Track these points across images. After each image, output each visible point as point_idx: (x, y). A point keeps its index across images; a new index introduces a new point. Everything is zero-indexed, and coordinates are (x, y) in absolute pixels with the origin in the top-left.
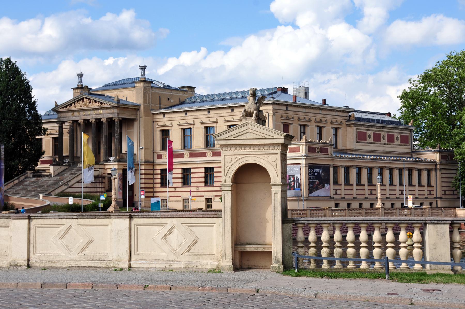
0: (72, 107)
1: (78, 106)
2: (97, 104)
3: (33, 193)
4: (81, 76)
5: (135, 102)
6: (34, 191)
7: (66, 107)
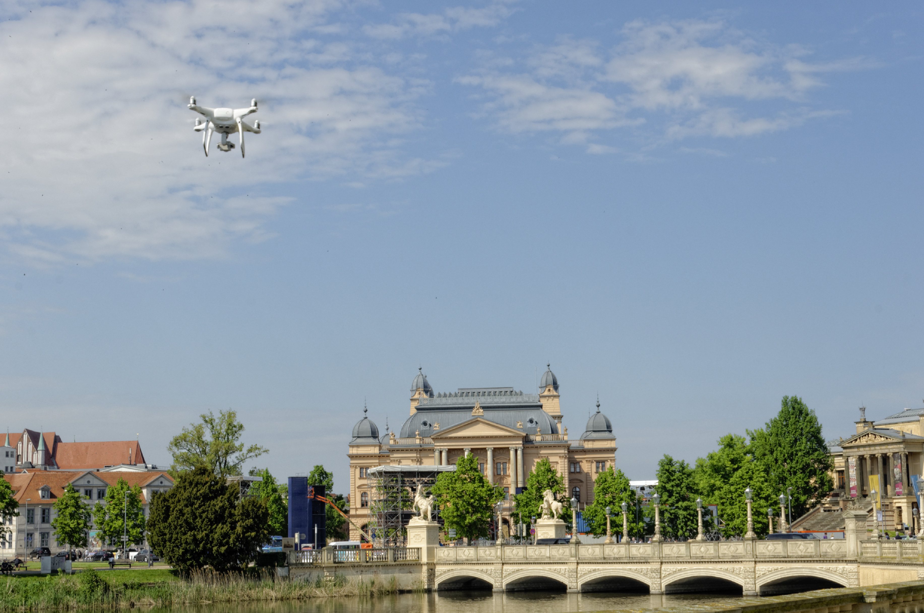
0: (857, 442)
1: (863, 441)
2: (883, 439)
3: (829, 527)
4: (863, 410)
5: (920, 435)
6: (828, 525)
7: (851, 442)
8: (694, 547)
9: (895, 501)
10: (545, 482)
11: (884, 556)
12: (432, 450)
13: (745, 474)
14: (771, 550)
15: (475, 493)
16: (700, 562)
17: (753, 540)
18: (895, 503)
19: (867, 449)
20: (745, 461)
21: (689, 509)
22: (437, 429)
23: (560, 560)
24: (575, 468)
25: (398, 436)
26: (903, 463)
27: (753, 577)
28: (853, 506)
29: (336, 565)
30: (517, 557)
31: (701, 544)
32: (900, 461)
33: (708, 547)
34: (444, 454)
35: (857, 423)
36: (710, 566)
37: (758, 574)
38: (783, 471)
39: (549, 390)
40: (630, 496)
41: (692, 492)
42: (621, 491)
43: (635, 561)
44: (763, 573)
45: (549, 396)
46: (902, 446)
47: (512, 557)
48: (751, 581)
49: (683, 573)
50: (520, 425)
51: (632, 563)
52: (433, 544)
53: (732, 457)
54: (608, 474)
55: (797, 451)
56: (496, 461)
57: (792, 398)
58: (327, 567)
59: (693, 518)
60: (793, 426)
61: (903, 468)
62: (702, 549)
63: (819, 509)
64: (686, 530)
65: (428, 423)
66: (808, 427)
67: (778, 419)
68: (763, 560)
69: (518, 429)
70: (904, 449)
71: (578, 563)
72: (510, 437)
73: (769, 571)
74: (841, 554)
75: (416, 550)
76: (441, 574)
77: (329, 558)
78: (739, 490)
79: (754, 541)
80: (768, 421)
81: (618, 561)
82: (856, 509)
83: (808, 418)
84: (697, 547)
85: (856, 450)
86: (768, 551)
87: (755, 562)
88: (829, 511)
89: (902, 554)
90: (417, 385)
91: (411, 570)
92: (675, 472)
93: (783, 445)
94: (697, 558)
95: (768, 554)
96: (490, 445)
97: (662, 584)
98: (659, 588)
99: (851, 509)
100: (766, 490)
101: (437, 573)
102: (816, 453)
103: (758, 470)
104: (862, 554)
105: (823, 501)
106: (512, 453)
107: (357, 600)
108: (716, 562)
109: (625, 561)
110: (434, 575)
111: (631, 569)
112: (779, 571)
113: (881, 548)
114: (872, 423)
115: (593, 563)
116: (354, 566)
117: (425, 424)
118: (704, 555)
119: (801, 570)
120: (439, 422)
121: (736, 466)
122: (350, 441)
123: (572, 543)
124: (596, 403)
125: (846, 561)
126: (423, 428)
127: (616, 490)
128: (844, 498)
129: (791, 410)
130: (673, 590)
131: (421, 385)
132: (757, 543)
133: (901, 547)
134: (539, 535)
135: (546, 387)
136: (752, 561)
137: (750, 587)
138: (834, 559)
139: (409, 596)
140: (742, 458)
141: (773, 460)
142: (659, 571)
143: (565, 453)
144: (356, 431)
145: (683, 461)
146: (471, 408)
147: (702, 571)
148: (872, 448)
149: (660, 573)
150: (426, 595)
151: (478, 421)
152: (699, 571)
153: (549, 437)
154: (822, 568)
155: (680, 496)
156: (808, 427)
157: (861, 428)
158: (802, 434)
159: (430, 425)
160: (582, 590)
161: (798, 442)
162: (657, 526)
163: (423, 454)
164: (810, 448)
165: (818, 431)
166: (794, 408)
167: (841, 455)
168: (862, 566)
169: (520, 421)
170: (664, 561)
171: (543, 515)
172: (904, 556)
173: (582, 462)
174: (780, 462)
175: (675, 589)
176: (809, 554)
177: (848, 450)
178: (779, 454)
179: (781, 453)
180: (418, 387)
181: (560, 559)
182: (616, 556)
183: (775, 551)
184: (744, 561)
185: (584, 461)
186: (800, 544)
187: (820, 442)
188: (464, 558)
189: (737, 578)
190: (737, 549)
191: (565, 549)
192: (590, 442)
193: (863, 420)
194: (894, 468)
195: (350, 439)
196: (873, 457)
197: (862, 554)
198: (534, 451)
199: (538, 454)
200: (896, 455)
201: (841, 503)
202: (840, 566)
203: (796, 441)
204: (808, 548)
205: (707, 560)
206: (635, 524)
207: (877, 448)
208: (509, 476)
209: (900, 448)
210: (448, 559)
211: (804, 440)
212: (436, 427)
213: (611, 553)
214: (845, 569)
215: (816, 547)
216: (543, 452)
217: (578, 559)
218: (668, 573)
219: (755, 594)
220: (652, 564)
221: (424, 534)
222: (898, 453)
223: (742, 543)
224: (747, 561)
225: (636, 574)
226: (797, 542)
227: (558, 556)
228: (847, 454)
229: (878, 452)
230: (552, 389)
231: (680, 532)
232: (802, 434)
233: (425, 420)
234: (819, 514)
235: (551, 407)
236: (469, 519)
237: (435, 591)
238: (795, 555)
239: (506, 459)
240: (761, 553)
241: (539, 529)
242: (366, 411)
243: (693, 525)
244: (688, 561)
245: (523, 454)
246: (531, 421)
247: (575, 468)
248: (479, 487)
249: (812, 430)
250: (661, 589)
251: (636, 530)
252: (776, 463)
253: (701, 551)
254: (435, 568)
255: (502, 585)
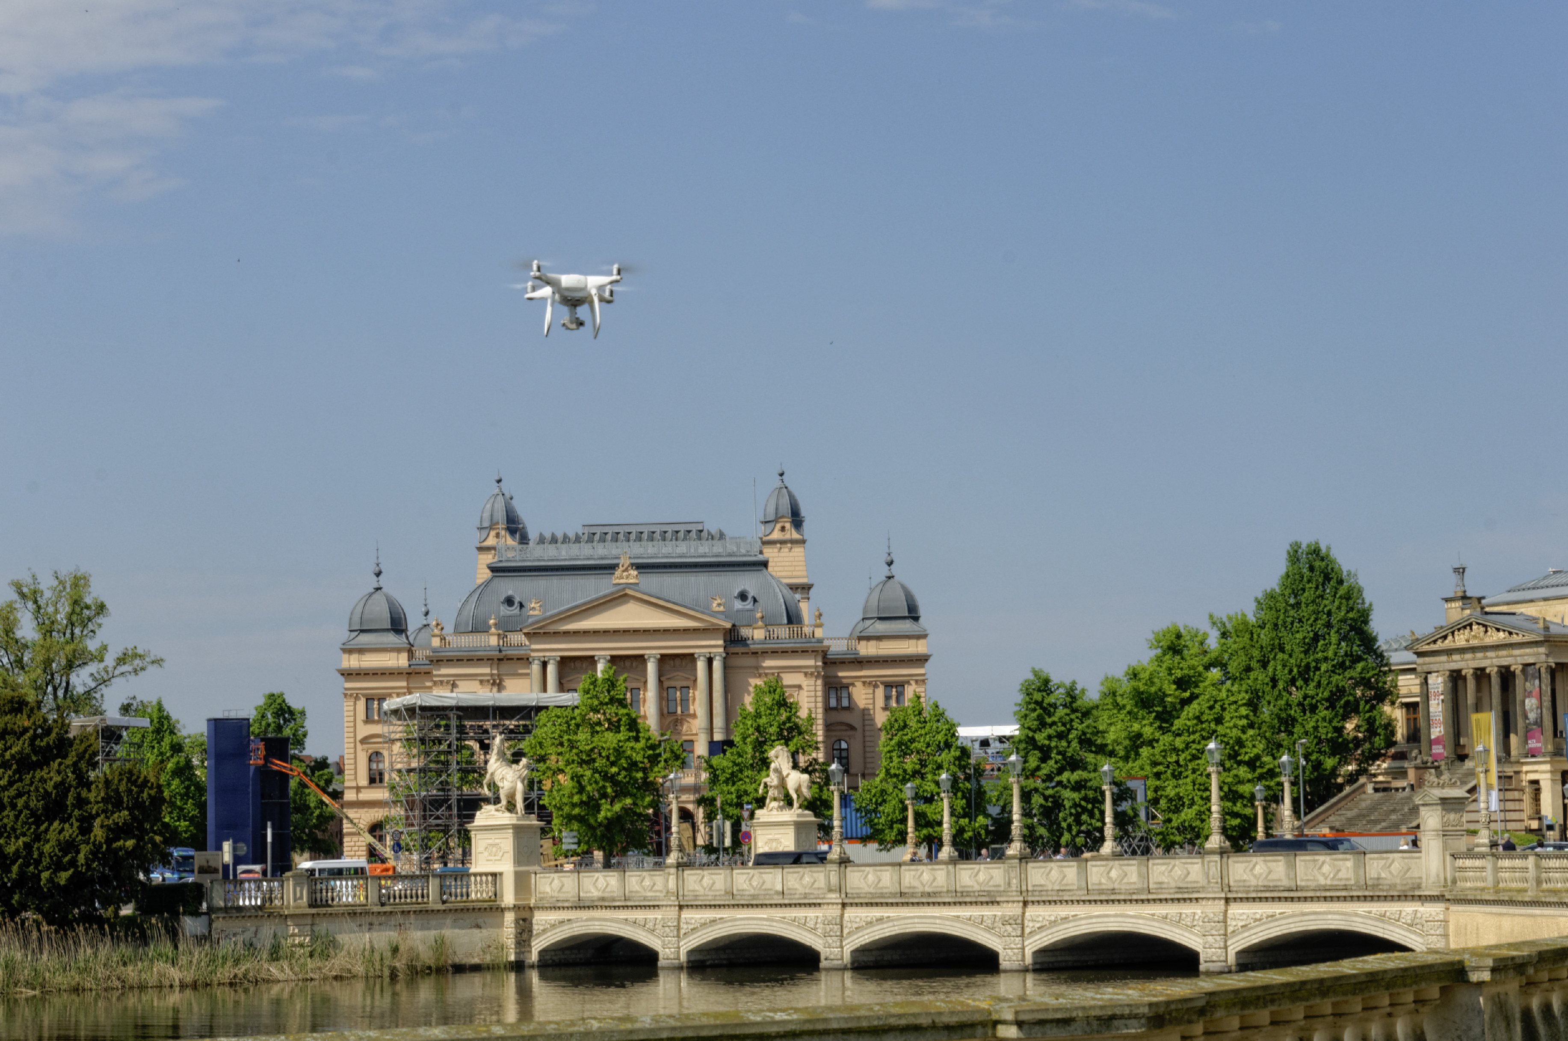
0: (1447, 641)
1: (1461, 639)
3: (1384, 824)
4: (1460, 571)
6: (1384, 821)
7: (1435, 642)
8: (1095, 869)
9: (1525, 768)
10: (773, 730)
11: (1501, 885)
12: (525, 660)
13: (1207, 711)
14: (1261, 874)
15: (619, 752)
16: (1107, 901)
17: (1222, 852)
18: (1527, 772)
19: (1468, 656)
20: (1206, 684)
21: (1085, 787)
22: (536, 613)
23: (805, 898)
24: (839, 700)
25: (449, 629)
26: (1543, 687)
27: (1222, 932)
28: (1436, 780)
29: (314, 911)
30: (711, 893)
31: (1111, 863)
32: (1537, 682)
33: (1124, 868)
34: (551, 669)
35: (1447, 600)
36: (1131, 910)
37: (1232, 925)
38: (1288, 705)
39: (783, 529)
40: (958, 759)
41: (1091, 751)
42: (940, 749)
43: (968, 899)
44: (1243, 923)
45: (783, 542)
46: (1542, 650)
47: (702, 892)
48: (1216, 941)
49: (1071, 925)
50: (719, 605)
51: (960, 903)
52: (529, 864)
53: (1179, 674)
54: (910, 712)
55: (1317, 661)
56: (666, 684)
57: (1308, 546)
58: (292, 916)
59: (1094, 807)
60: (1311, 608)
61: (1544, 698)
62: (1114, 874)
63: (1363, 785)
64: (1079, 832)
65: (517, 600)
66: (1343, 608)
67: (1278, 590)
68: (1244, 895)
69: (714, 614)
70: (1547, 655)
71: (844, 905)
72: (696, 630)
73: (1256, 920)
74: (1410, 881)
75: (490, 878)
76: (544, 931)
77: (298, 895)
78: (1194, 746)
79: (1225, 856)
80: (1260, 596)
81: (930, 900)
82: (1443, 787)
83: (1342, 591)
84: (1102, 869)
85: (1444, 658)
86: (1255, 876)
87: (1227, 900)
88: (1385, 790)
89: (1539, 882)
90: (492, 515)
91: (480, 921)
92: (1054, 706)
93: (1288, 647)
94: (1101, 892)
95: (1254, 882)
96: (652, 649)
97: (1027, 949)
98: (1020, 957)
99: (1432, 786)
100: (1250, 745)
101: (536, 928)
102: (1360, 666)
103: (1236, 702)
104: (1454, 881)
105: (1373, 769)
106: (701, 665)
107: (360, 986)
108: (1143, 901)
109: (947, 900)
110: (531, 931)
111: (958, 917)
112: (1277, 920)
113: (1497, 870)
114: (1479, 600)
115: (877, 904)
116: (354, 913)
117: (509, 601)
118: (1116, 886)
119: (1325, 917)
120: (541, 598)
121: (1187, 694)
122: (344, 640)
123: (832, 862)
124: (885, 558)
125: (1420, 896)
126: (505, 610)
127: (928, 745)
128: (1419, 761)
129: (1305, 571)
130: (1049, 963)
131: (501, 516)
132: (1230, 860)
133: (1538, 866)
134: (759, 844)
135: (776, 521)
136: (1220, 898)
137: (1214, 954)
138: (1396, 894)
139: (477, 979)
140: (1200, 675)
141: (1267, 680)
142: (1019, 921)
143: (816, 667)
144: (356, 618)
145: (1074, 683)
146: (613, 567)
147: (1112, 919)
148: (1479, 655)
149: (1023, 924)
150: (512, 976)
151: (626, 595)
152: (1106, 920)
153: (783, 632)
154: (1370, 912)
155: (1064, 758)
156: (1343, 608)
157: (1456, 612)
158: (1329, 625)
159: (521, 606)
160: (853, 963)
161: (1321, 642)
162: (1016, 824)
163: (505, 667)
164: (1346, 655)
165: (1364, 617)
166: (1312, 569)
167: (1412, 670)
168: (1454, 908)
169: (718, 595)
170: (1030, 899)
171: (768, 801)
172: (1544, 886)
173: (853, 685)
174: (1281, 685)
175: (1053, 959)
176: (1343, 883)
177: (1427, 659)
178: (1279, 667)
179: (1284, 666)
180: (495, 520)
181: (806, 896)
182: (927, 889)
183: (1270, 877)
184: (1203, 899)
185: (859, 684)
186: (1323, 863)
187: (1368, 642)
188: (596, 894)
189: (1186, 934)
190: (1188, 873)
191: (815, 875)
192: (873, 643)
193: (1460, 594)
194: (1525, 697)
195: (345, 635)
196: (1481, 674)
197: (1454, 881)
198: (749, 661)
199: (757, 668)
200: (1530, 670)
201: (1411, 773)
202: (1408, 908)
203: (1316, 638)
204: (1339, 871)
205: (1122, 897)
206: (967, 820)
207: (1490, 654)
208: (694, 716)
209: (1538, 656)
210: (562, 896)
211: (1334, 638)
212: (535, 610)
213: (916, 883)
214: (1419, 915)
215: (1356, 867)
216: (768, 663)
217: (843, 896)
218: (1038, 925)
219: (1226, 970)
220: (1005, 905)
221: (507, 842)
222: (1534, 664)
223: (1199, 860)
224: (1208, 899)
225: (969, 928)
226: (1317, 857)
227: (801, 890)
228: (1426, 668)
229: (1491, 662)
230: (788, 525)
231: (1066, 838)
232: (1329, 625)
233: (510, 593)
234: (1363, 796)
235: (787, 565)
236: (606, 811)
237: (532, 966)
238: (1312, 884)
239: (688, 679)
240: (1240, 881)
241: (759, 832)
242: (378, 574)
243: (1093, 821)
244: (1083, 898)
245: (726, 668)
246: (743, 596)
247: (839, 700)
248: (628, 740)
249: (1351, 615)
250: (1023, 960)
251: (970, 834)
252: (1274, 686)
253: (1110, 878)
254: (532, 916)
255: (679, 952)
